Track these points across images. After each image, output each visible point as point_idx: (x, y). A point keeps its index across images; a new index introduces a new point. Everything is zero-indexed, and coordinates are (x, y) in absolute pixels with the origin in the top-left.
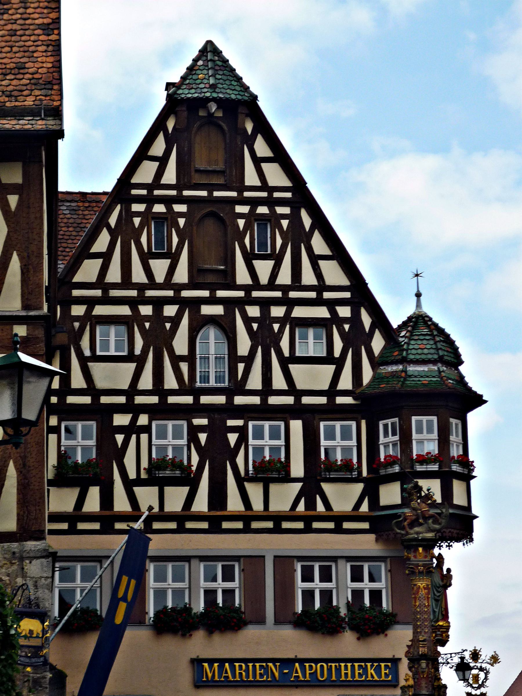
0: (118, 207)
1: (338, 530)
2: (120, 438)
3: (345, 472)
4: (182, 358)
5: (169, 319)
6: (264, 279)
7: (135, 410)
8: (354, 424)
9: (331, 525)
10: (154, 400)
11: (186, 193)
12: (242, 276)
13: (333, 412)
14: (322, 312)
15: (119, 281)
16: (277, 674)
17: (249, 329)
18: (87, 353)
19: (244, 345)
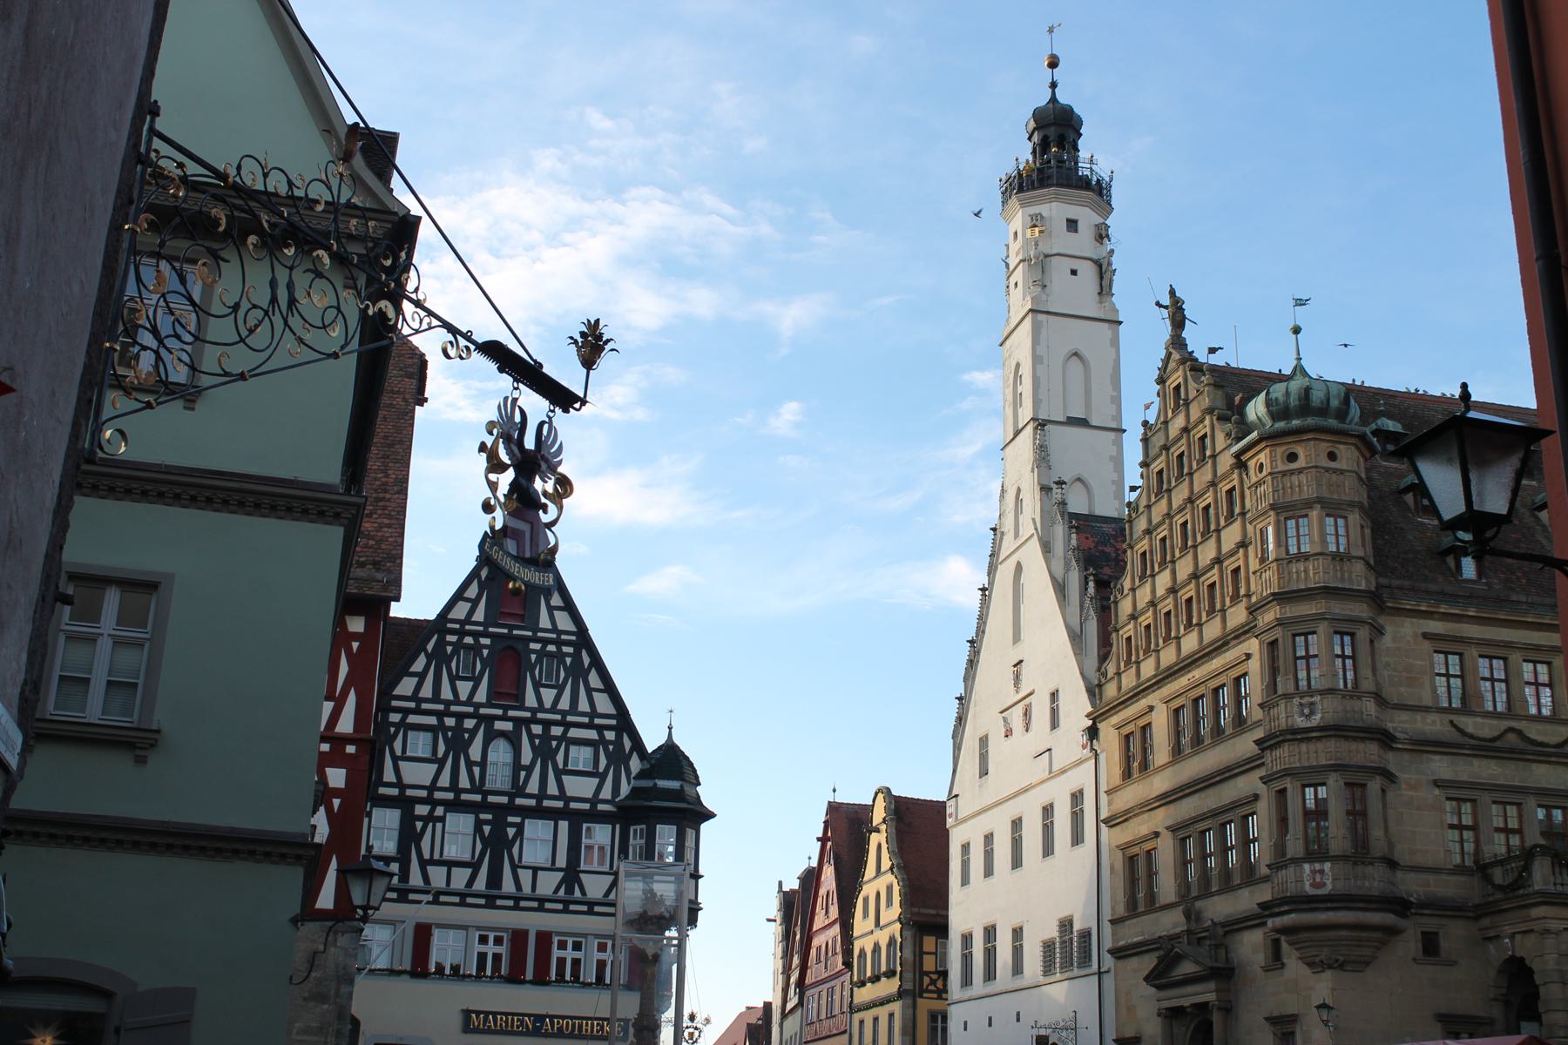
1: (590, 912)
2: (419, 825)
4: (476, 764)
5: (467, 730)
6: (548, 704)
7: (434, 803)
9: (585, 908)
10: (450, 796)
12: (530, 700)
14: (592, 734)
18: (399, 752)
19: (527, 756)
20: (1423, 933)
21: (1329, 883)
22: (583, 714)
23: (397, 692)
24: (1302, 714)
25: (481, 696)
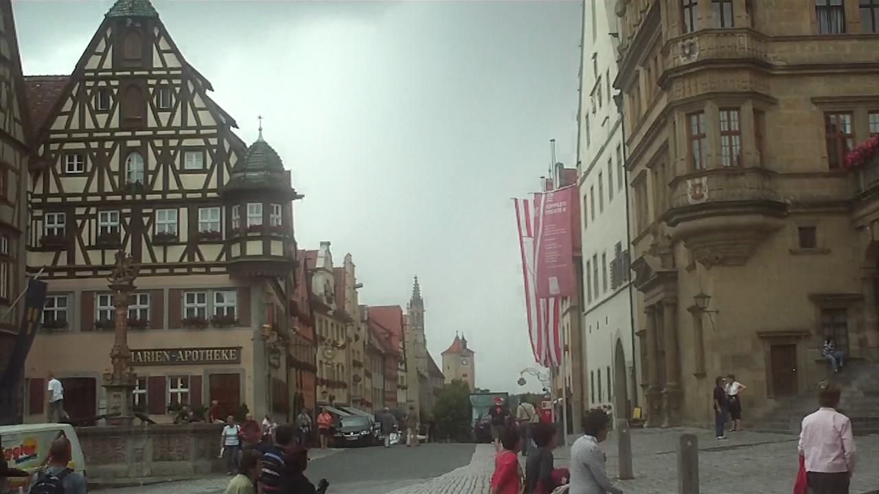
0: (78, 84)
1: (208, 272)
2: (79, 222)
3: (212, 238)
4: (115, 173)
5: (108, 150)
6: (164, 123)
8: (219, 209)
9: (203, 270)
10: (98, 198)
11: (117, 74)
12: (151, 122)
13: (205, 202)
14: (200, 142)
15: (78, 128)
16: (168, 357)
17: (156, 154)
18: (59, 172)
20: (800, 229)
21: (706, 196)
22: (191, 128)
23: (54, 127)
24: (684, 55)
25: (115, 123)
